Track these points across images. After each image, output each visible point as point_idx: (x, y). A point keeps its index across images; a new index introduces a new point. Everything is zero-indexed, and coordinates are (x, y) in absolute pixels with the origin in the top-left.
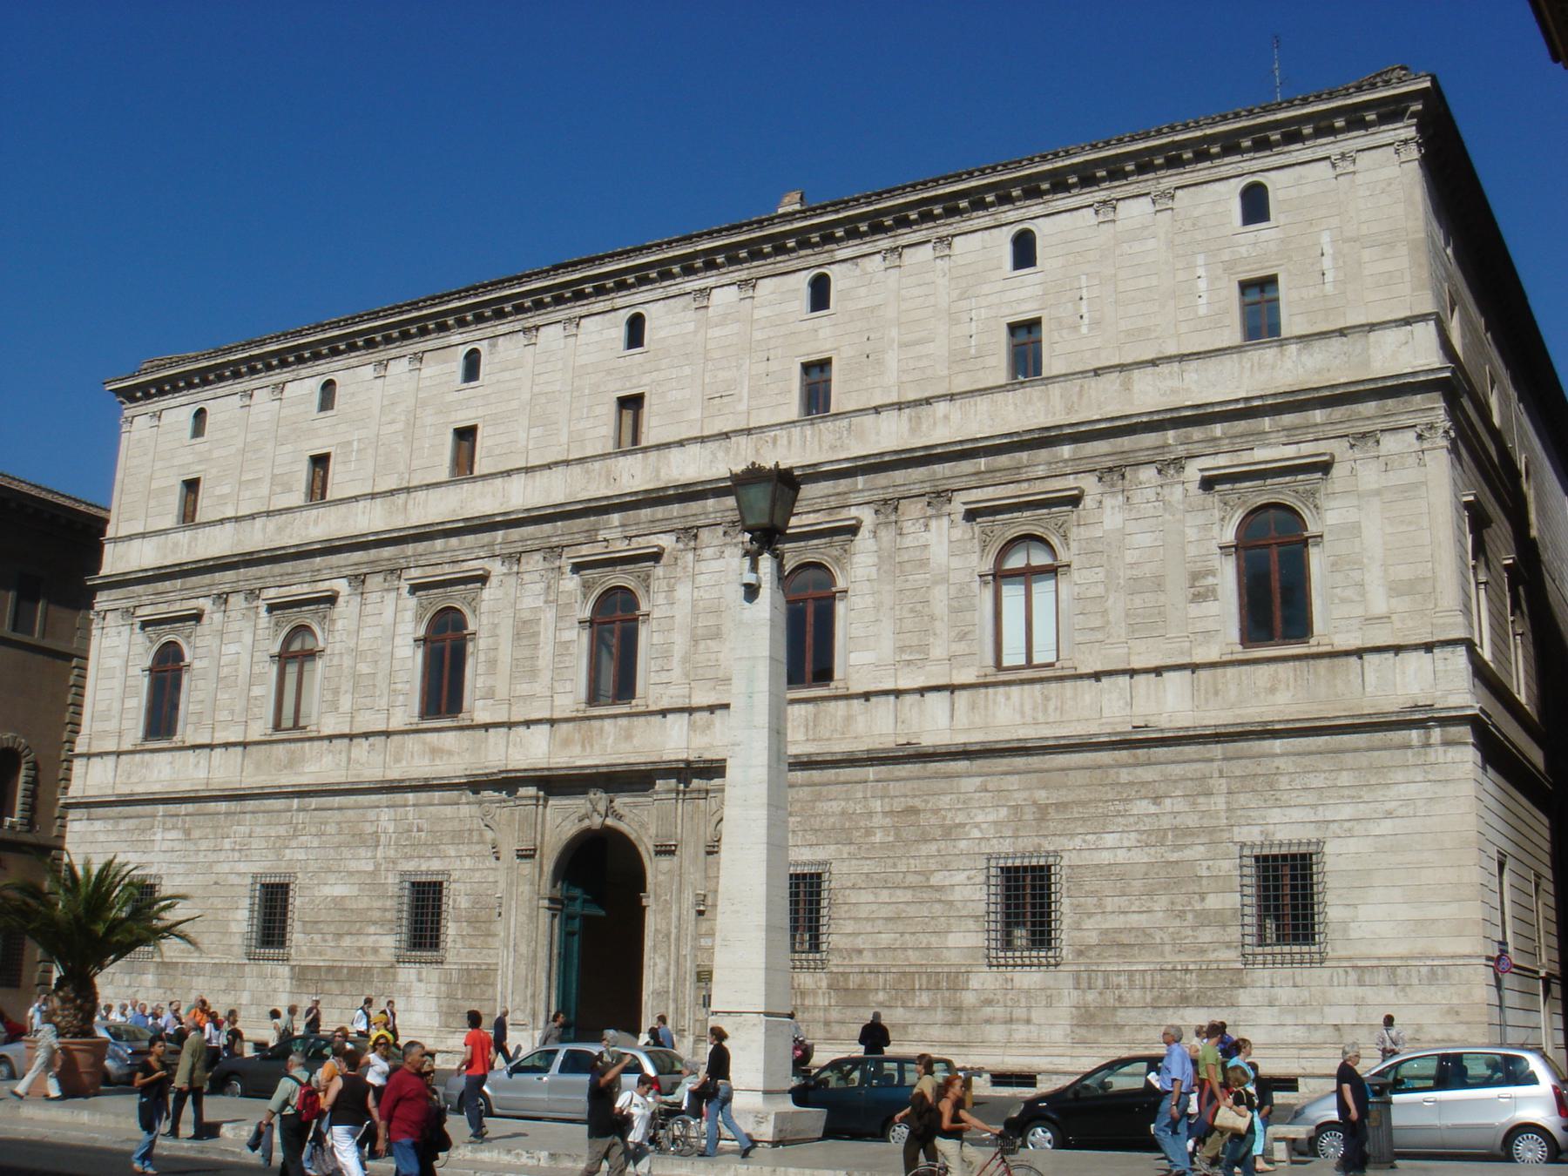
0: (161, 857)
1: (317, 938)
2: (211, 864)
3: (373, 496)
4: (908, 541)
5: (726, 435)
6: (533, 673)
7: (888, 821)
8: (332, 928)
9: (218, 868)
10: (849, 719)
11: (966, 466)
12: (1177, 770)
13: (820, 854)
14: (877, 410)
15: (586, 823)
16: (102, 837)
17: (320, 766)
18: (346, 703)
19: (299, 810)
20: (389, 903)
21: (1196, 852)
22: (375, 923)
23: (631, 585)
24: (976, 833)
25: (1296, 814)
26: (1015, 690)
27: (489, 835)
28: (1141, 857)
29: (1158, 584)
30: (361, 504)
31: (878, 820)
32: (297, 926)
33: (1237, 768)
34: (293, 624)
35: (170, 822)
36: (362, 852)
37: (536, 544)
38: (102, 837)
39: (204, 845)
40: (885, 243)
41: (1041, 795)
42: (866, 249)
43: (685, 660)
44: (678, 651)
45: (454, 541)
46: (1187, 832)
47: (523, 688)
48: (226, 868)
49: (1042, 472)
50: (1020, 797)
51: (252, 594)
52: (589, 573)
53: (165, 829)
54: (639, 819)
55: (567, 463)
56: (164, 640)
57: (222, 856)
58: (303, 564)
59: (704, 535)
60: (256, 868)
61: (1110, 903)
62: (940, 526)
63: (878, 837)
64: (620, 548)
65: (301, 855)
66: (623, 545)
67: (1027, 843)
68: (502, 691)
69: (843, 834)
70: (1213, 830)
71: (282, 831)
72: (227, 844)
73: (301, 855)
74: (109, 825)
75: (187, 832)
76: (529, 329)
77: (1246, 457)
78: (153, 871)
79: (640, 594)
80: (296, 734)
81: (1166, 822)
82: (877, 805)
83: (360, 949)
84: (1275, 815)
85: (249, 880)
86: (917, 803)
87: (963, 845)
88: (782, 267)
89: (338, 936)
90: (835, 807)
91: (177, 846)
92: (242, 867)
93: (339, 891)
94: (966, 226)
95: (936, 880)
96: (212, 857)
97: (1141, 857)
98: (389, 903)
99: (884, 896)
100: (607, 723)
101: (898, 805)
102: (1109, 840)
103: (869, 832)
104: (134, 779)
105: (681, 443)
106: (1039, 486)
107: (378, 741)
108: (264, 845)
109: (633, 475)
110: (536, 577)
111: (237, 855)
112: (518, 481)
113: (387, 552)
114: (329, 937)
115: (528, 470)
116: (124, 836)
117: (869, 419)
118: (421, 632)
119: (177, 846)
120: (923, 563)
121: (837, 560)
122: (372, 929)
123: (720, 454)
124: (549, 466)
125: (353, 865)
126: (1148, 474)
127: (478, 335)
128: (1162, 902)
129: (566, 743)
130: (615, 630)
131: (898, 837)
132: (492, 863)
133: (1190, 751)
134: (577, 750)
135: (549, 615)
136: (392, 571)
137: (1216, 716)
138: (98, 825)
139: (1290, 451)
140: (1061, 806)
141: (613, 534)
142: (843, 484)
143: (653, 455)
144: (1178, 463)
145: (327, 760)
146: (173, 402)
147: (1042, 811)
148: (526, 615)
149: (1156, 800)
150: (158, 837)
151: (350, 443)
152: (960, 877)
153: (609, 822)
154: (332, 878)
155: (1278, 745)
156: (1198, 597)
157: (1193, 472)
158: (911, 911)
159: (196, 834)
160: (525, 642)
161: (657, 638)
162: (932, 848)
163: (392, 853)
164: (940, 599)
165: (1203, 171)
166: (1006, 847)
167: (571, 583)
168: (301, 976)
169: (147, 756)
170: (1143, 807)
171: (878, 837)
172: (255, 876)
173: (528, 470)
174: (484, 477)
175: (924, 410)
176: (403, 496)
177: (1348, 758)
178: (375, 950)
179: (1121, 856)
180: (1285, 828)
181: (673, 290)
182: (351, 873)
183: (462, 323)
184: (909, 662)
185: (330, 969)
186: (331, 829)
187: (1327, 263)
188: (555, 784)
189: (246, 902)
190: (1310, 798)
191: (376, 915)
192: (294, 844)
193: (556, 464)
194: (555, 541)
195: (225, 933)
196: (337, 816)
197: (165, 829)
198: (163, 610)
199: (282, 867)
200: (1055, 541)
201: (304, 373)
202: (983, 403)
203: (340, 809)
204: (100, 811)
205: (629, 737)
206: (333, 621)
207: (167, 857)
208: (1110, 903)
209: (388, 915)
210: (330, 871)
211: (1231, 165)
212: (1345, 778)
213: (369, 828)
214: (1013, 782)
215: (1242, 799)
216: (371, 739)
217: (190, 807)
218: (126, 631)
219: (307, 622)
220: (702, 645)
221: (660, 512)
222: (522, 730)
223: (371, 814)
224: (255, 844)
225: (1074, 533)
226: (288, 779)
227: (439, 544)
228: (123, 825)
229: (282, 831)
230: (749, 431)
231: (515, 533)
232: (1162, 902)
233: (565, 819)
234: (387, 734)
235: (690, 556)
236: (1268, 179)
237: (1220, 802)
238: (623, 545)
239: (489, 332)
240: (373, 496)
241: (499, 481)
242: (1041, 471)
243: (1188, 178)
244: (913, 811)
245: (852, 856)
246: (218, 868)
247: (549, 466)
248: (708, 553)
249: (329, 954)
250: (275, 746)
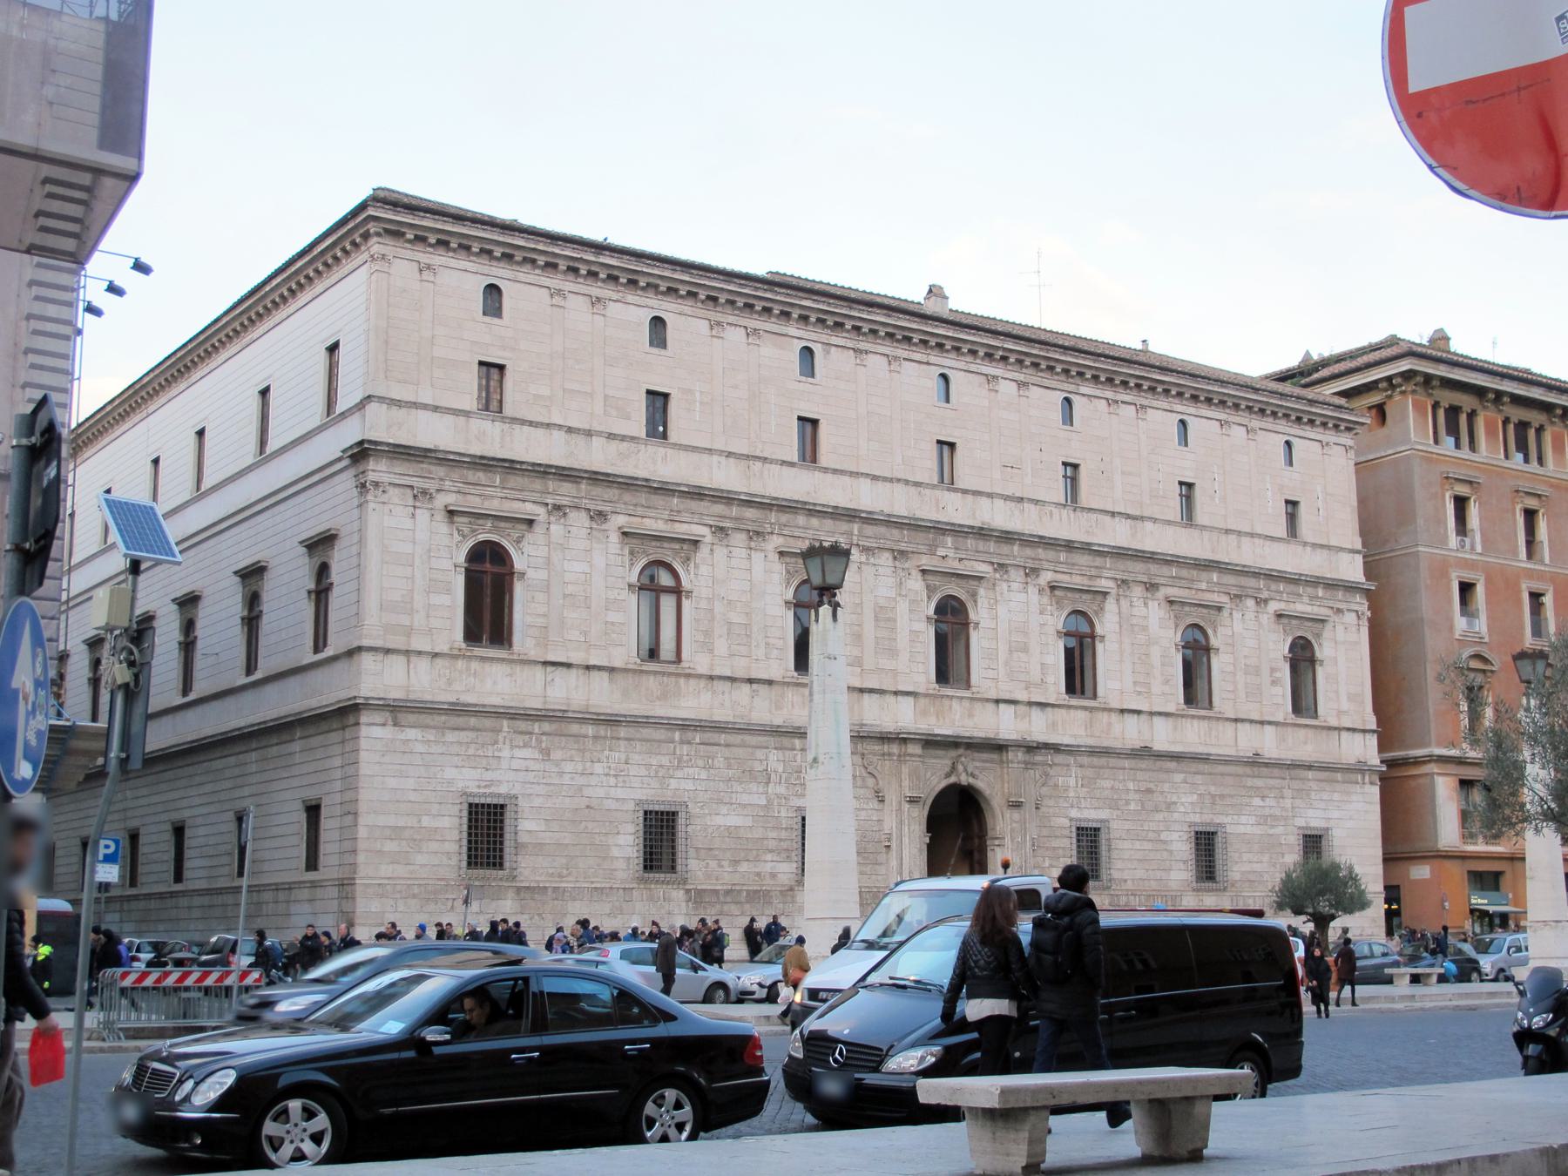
0: (511, 776)
1: (713, 864)
2: (580, 788)
3: (730, 455)
4: (1135, 611)
5: (1021, 500)
6: (893, 652)
7: (1137, 797)
8: (728, 855)
9: (586, 792)
10: (1110, 724)
11: (1165, 570)
12: (1272, 782)
13: (1103, 814)
14: (1113, 514)
15: (953, 779)
16: (420, 748)
17: (693, 703)
18: (721, 646)
19: (682, 742)
20: (784, 834)
21: (1279, 830)
22: (771, 851)
23: (963, 597)
24: (1182, 809)
25: (1319, 813)
26: (1195, 722)
27: (870, 782)
28: (1258, 830)
29: (1257, 671)
30: (715, 458)
31: (1131, 796)
32: (692, 852)
33: (1296, 784)
34: (652, 558)
35: (520, 740)
36: (753, 787)
37: (889, 544)
38: (420, 748)
39: (569, 767)
40: (1109, 394)
41: (1213, 789)
42: (1098, 393)
43: (1006, 663)
44: (1002, 656)
45: (815, 522)
46: (1275, 818)
47: (886, 663)
48: (601, 792)
49: (1207, 588)
50: (1202, 789)
51: (601, 516)
52: (935, 581)
53: (512, 747)
54: (986, 778)
55: (907, 482)
56: (481, 537)
57: (594, 780)
58: (658, 500)
59: (1013, 573)
60: (640, 794)
61: (1246, 857)
62: (1153, 605)
63: (1132, 807)
64: (953, 565)
65: (689, 785)
66: (956, 564)
67: (1207, 818)
68: (869, 663)
69: (1113, 805)
70: (1286, 818)
71: (665, 761)
72: (598, 768)
73: (689, 785)
74: (430, 735)
75: (546, 753)
76: (861, 352)
77: (1292, 606)
78: (503, 790)
79: (969, 606)
80: (672, 668)
81: (1267, 811)
82: (1131, 786)
83: (758, 874)
84: (1311, 813)
85: (631, 806)
86: (1151, 786)
87: (1176, 815)
88: (1047, 383)
89: (736, 862)
90: (1107, 784)
91: (533, 765)
92: (620, 793)
93: (734, 821)
94: (1155, 403)
95: (1163, 836)
96: (581, 780)
97: (1258, 830)
98: (784, 834)
99: (1138, 845)
100: (955, 704)
101: (1143, 786)
102: (1244, 819)
103: (1127, 803)
104: (457, 686)
105: (990, 495)
106: (1201, 595)
107: (763, 689)
108: (643, 772)
109: (955, 510)
110: (889, 571)
111: (612, 781)
112: (865, 484)
113: (750, 513)
114: (725, 863)
115: (875, 478)
116: (455, 749)
117: (1108, 518)
118: (790, 595)
119: (533, 765)
120: (1145, 628)
121: (1096, 613)
122: (769, 857)
123: (1017, 513)
124: (891, 480)
125: (745, 799)
126: (1250, 603)
127: (813, 336)
128: (1266, 858)
129: (924, 713)
130: (952, 626)
131: (1143, 807)
132: (875, 804)
133: (1276, 771)
134: (933, 720)
135: (903, 607)
136: (757, 533)
137: (1288, 755)
138: (412, 734)
139: (1308, 609)
140: (1222, 796)
141: (948, 555)
142: (1099, 561)
143: (970, 497)
144: (1266, 601)
145: (706, 697)
146: (453, 263)
147: (1213, 796)
148: (882, 602)
149: (1263, 798)
150: (506, 753)
151: (690, 392)
152: (1175, 836)
153: (971, 780)
154: (724, 809)
155: (1310, 774)
156: (1274, 683)
157: (1273, 606)
158: (1152, 855)
159: (557, 755)
160: (882, 624)
161: (985, 644)
162: (1159, 816)
163: (782, 790)
164: (1156, 653)
165: (1268, 423)
166: (1197, 819)
167: (916, 584)
168: (698, 897)
169: (475, 665)
170: (1257, 801)
171: (1132, 807)
172: (639, 803)
173: (875, 478)
174: (826, 470)
175: (1139, 523)
176: (759, 464)
177: (1338, 786)
178: (773, 876)
179: (1249, 830)
180: (1314, 819)
181: (973, 367)
182: (744, 806)
183: (804, 319)
184: (1140, 693)
185: (728, 892)
186: (719, 762)
187: (1320, 504)
188: (932, 743)
189: (631, 828)
190: (1322, 805)
191: (772, 844)
192: (679, 774)
193: (899, 480)
194: (903, 546)
195: (604, 858)
196: (726, 752)
197: (512, 747)
198: (473, 503)
199: (668, 796)
200: (1210, 632)
201: (630, 298)
202: (1170, 530)
203: (727, 745)
204: (412, 718)
205: (971, 716)
206: (696, 566)
207: (521, 776)
208: (1246, 857)
209: (784, 845)
210: (720, 802)
211: (1282, 426)
212: (1336, 796)
213: (758, 767)
214: (1199, 779)
215: (1298, 802)
216: (755, 686)
217: (546, 727)
218: (423, 515)
219: (668, 560)
220: (1015, 655)
221: (981, 545)
222: (890, 699)
223: (760, 754)
224: (633, 771)
225: (1220, 629)
226: (660, 710)
227: (801, 520)
228: (451, 736)
229: (665, 761)
230: (1037, 502)
231: (870, 530)
232: (1266, 858)
233: (934, 776)
234: (770, 682)
235: (1005, 585)
236: (1295, 441)
237: (1288, 803)
238: (956, 564)
239: (824, 338)
240: (730, 455)
241: (846, 479)
242: (1204, 586)
243: (1264, 425)
244: (1149, 791)
245: (1118, 818)
246: (586, 792)
247: (891, 480)
248: (1015, 586)
249: (727, 878)
250: (644, 677)
